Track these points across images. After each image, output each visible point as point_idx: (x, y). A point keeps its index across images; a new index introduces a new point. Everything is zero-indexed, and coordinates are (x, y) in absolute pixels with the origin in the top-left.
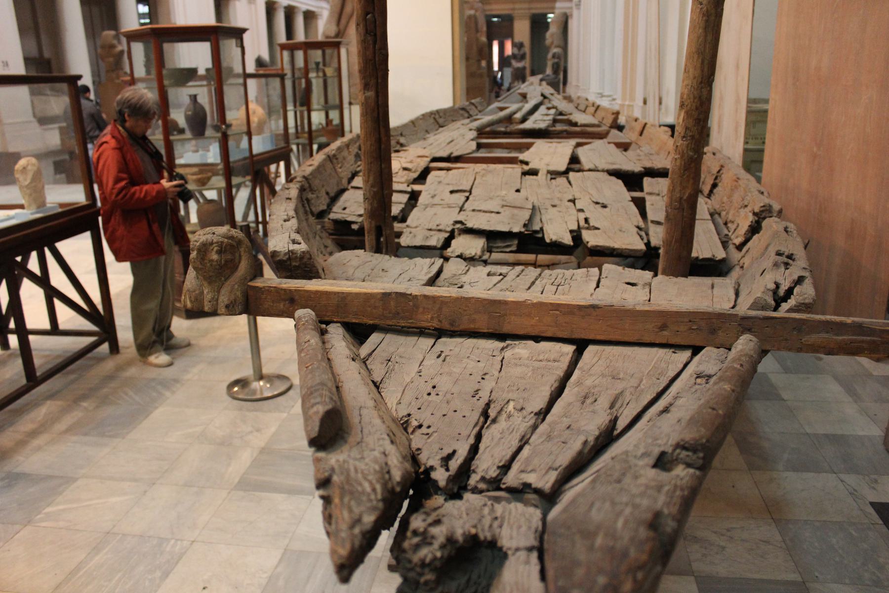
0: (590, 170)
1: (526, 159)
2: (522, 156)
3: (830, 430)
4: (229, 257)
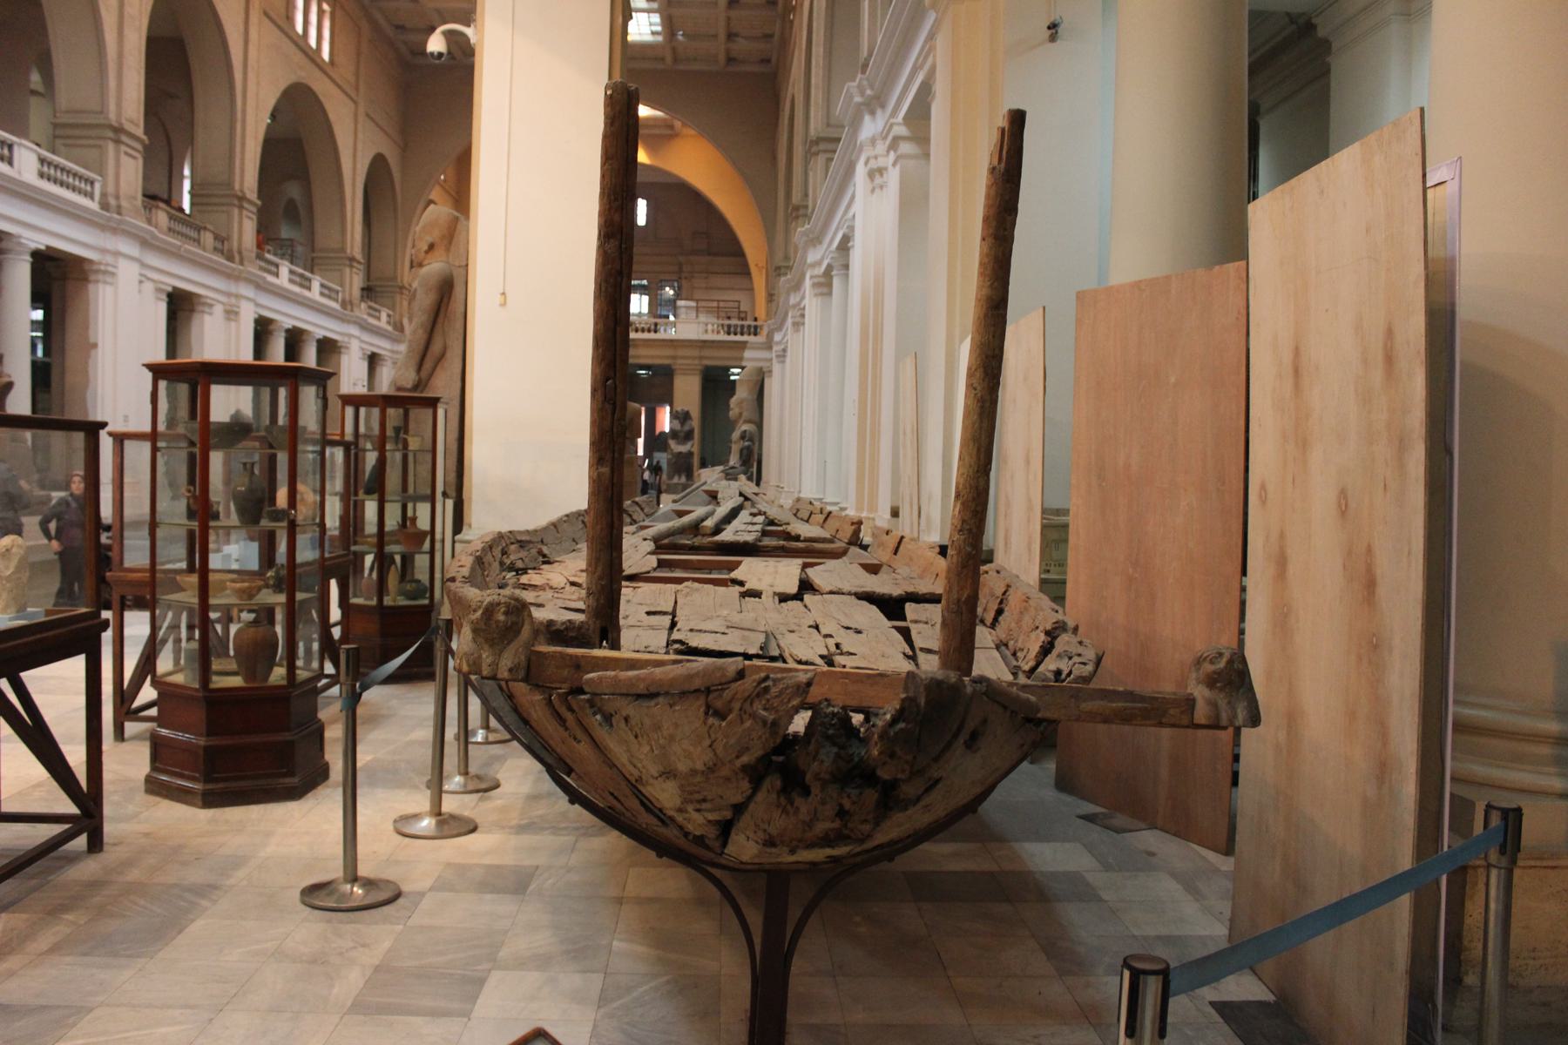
0: (831, 593)
1: (740, 578)
2: (736, 574)
3: (1164, 931)
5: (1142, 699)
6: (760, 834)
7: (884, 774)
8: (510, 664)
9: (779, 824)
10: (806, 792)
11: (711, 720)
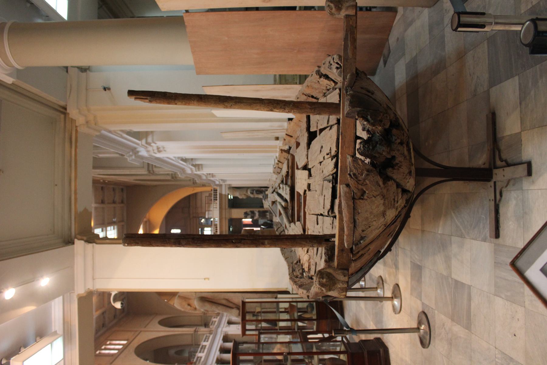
0: (307, 158)
1: (303, 191)
2: (302, 193)
3: (427, 32)
4: (325, 275)
5: (346, 35)
6: (407, 177)
7: (387, 126)
8: (343, 276)
9: (404, 169)
10: (394, 157)
11: (365, 197)
